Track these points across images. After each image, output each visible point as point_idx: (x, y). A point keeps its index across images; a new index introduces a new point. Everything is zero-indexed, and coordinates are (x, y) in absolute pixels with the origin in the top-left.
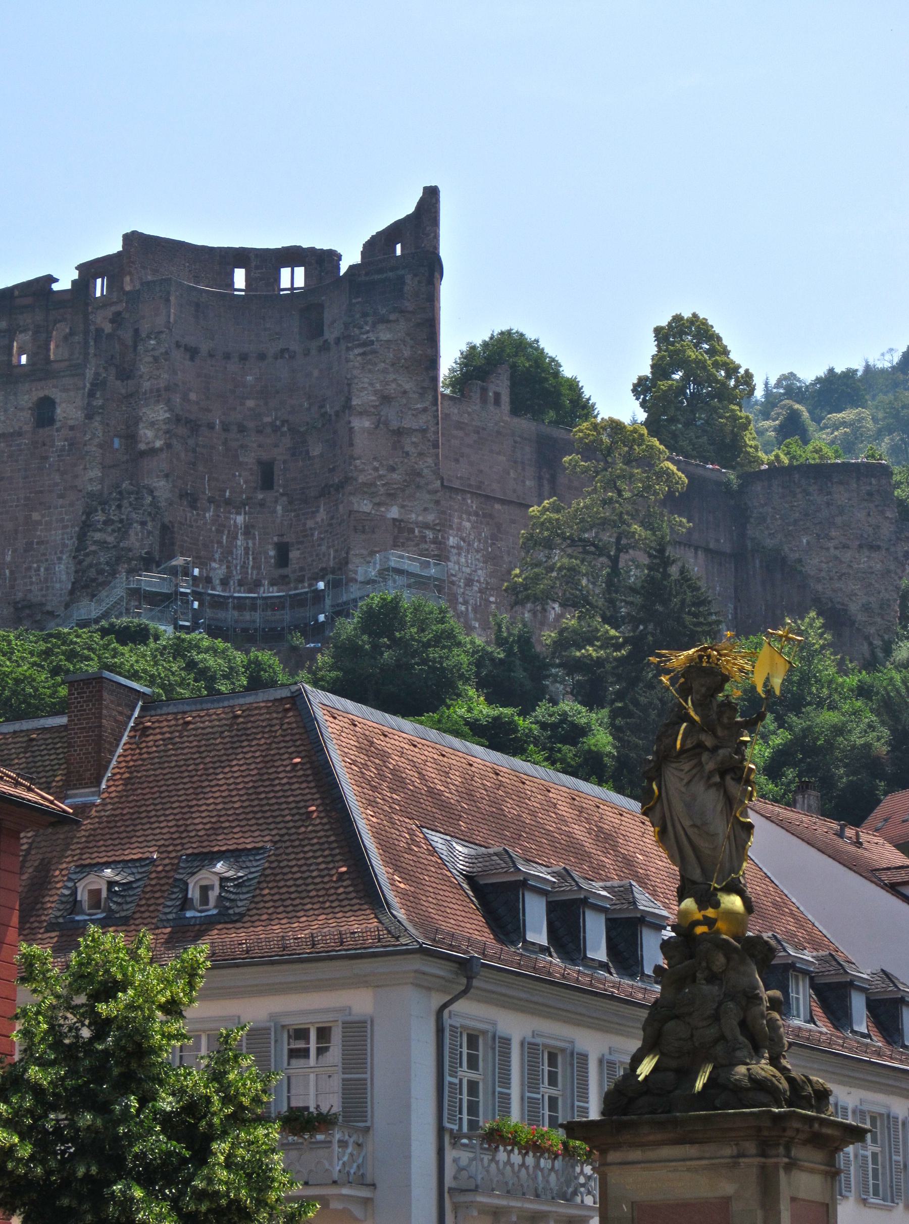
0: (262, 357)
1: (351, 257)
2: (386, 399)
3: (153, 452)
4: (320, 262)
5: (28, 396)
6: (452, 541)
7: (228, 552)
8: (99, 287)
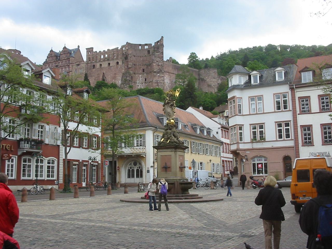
0: (143, 57)
1: (153, 45)
2: (157, 61)
3: (130, 68)
5: (116, 61)
6: (165, 78)
7: (139, 80)
8: (124, 49)
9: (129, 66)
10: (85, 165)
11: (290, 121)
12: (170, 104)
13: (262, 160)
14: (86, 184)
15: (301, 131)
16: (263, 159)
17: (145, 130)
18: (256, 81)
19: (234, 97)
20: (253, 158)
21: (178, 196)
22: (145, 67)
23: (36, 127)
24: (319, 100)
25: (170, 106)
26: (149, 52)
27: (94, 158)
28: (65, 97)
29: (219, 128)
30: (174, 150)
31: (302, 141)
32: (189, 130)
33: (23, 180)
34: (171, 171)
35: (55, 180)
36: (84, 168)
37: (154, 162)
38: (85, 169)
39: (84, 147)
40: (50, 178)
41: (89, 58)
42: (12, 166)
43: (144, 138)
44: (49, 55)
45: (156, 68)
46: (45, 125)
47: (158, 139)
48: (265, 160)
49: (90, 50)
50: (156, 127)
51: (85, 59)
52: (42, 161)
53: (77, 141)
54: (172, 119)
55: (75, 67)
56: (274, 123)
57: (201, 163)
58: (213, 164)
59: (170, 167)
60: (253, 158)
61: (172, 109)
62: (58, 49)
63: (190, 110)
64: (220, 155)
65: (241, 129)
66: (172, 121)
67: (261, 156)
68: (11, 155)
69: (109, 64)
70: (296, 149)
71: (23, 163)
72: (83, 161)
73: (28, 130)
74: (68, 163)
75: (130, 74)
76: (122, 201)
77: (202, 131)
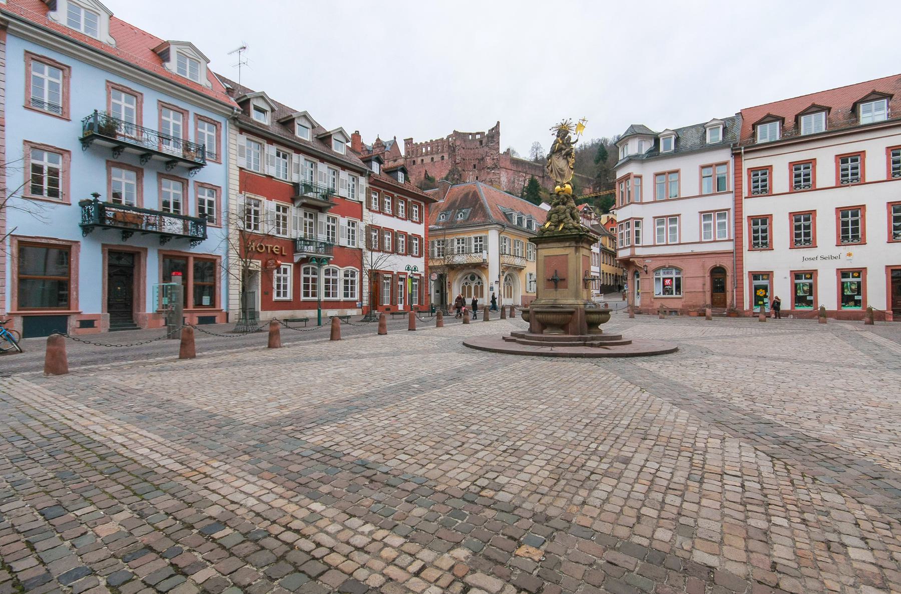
1: (487, 133)
4: (482, 134)
10: (401, 279)
11: (728, 210)
12: (564, 152)
13: (671, 273)
14: (404, 307)
15: (749, 225)
16: (674, 271)
17: (488, 230)
18: (667, 145)
19: (627, 177)
20: (657, 270)
22: (476, 162)
23: (323, 218)
24: (791, 170)
26: (481, 142)
28: (369, 175)
30: (573, 244)
31: (750, 242)
33: (304, 301)
34: (566, 287)
35: (355, 302)
36: (400, 283)
40: (350, 298)
41: (407, 152)
42: (285, 279)
43: (486, 242)
45: (489, 161)
46: (338, 217)
48: (677, 274)
49: (408, 142)
51: (403, 153)
52: (335, 272)
54: (568, 183)
56: (698, 214)
59: (564, 280)
60: (657, 270)
61: (568, 162)
65: (637, 224)
66: (568, 186)
67: (672, 267)
68: (279, 262)
69: (432, 159)
70: (737, 254)
71: (303, 276)
72: (399, 273)
73: (311, 224)
74: (375, 275)
75: (458, 171)
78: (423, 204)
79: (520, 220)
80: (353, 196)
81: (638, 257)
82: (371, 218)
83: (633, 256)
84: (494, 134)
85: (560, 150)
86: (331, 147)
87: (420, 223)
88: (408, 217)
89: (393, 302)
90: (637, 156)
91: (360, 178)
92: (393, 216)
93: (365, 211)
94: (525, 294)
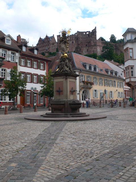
1: (91, 31)
2: (93, 40)
9: (79, 43)
19: (127, 49)
21: (67, 115)
25: (64, 42)
27: (35, 88)
29: (122, 72)
30: (65, 77)
32: (104, 72)
34: (63, 94)
36: (35, 95)
37: (79, 91)
38: (35, 96)
39: (35, 82)
44: (39, 40)
45: (93, 44)
46: (7, 69)
47: (82, 77)
50: (81, 70)
51: (57, 41)
53: (29, 79)
54: (66, 53)
55: (52, 45)
57: (111, 92)
58: (119, 92)
59: (62, 91)
62: (43, 37)
63: (106, 61)
64: (123, 87)
65: (132, 68)
66: (66, 55)
76: (26, 119)
77: (112, 73)
78: (45, 62)
79: (90, 68)
80: (13, 61)
81: (132, 82)
82: (21, 69)
83: (131, 82)
84: (94, 32)
85: (62, 41)
86: (5, 42)
87: (44, 70)
88: (38, 67)
89: (32, 102)
90: (130, 40)
91: (16, 53)
92: (31, 67)
93: (19, 67)
94: (93, 99)
